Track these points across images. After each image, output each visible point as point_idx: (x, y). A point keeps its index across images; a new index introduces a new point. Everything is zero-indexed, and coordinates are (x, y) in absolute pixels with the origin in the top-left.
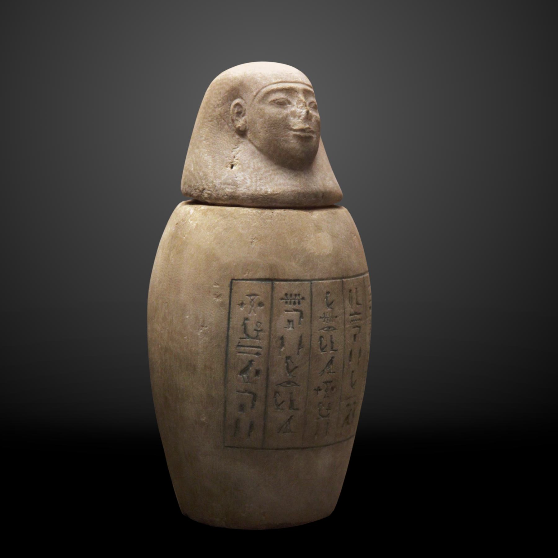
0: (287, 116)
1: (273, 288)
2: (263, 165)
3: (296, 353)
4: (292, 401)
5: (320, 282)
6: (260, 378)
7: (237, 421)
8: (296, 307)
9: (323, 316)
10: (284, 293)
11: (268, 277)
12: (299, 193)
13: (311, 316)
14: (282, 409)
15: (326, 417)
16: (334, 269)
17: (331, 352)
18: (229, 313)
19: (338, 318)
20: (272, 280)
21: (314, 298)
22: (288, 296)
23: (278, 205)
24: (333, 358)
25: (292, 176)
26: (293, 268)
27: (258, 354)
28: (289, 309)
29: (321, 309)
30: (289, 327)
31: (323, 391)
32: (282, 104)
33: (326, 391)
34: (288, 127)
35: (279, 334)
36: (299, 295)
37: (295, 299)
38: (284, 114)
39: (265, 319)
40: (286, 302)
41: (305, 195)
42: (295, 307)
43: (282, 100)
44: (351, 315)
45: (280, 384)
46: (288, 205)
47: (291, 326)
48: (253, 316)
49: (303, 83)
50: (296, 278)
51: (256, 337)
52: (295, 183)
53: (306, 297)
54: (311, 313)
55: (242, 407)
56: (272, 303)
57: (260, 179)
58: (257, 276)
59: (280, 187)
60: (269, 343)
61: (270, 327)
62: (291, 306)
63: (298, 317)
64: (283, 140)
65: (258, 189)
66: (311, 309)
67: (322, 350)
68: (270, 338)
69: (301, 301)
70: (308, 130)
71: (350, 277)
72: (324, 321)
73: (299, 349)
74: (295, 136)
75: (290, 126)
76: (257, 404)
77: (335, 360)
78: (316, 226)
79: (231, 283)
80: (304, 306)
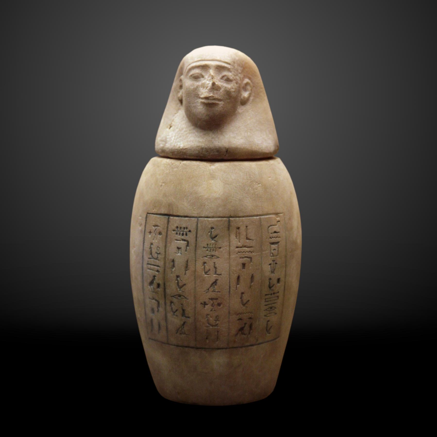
0: (197, 87)
1: (168, 222)
2: (185, 126)
3: (184, 273)
4: (184, 310)
5: (206, 219)
6: (160, 290)
7: (152, 320)
8: (184, 237)
9: (206, 246)
10: (175, 226)
11: (166, 212)
12: (202, 149)
13: (196, 246)
14: (177, 316)
15: (215, 326)
16: (220, 209)
17: (214, 275)
18: (144, 238)
19: (222, 249)
20: (169, 215)
21: (200, 233)
22: (179, 229)
23: (188, 157)
24: (216, 280)
25: (201, 134)
26: (184, 207)
27: (158, 271)
28: (178, 239)
29: (204, 240)
30: (179, 253)
31: (208, 305)
32: (196, 78)
33: (212, 306)
34: (197, 96)
35: (171, 258)
36: (187, 228)
37: (183, 231)
38: (195, 87)
39: (162, 245)
40: (177, 233)
41: (208, 150)
42: (183, 237)
43: (196, 75)
44: (237, 247)
45: (173, 296)
46: (195, 158)
47: (180, 252)
48: (155, 242)
49: (220, 61)
50: (186, 215)
51: (156, 259)
52: (201, 140)
53: (192, 230)
54: (196, 244)
55: (153, 310)
56: (167, 233)
57: (180, 137)
58: (159, 212)
59: (189, 143)
60: (165, 263)
61: (165, 252)
62: (179, 237)
63: (185, 246)
64: (194, 106)
65: (176, 145)
66: (196, 240)
67: (206, 273)
68: (165, 260)
69: (188, 233)
70: (211, 98)
71: (239, 217)
72: (207, 250)
73: (186, 270)
74: (202, 102)
75: (199, 95)
76: (161, 309)
77: (218, 282)
78: (211, 175)
79: (147, 215)
80: (191, 237)
